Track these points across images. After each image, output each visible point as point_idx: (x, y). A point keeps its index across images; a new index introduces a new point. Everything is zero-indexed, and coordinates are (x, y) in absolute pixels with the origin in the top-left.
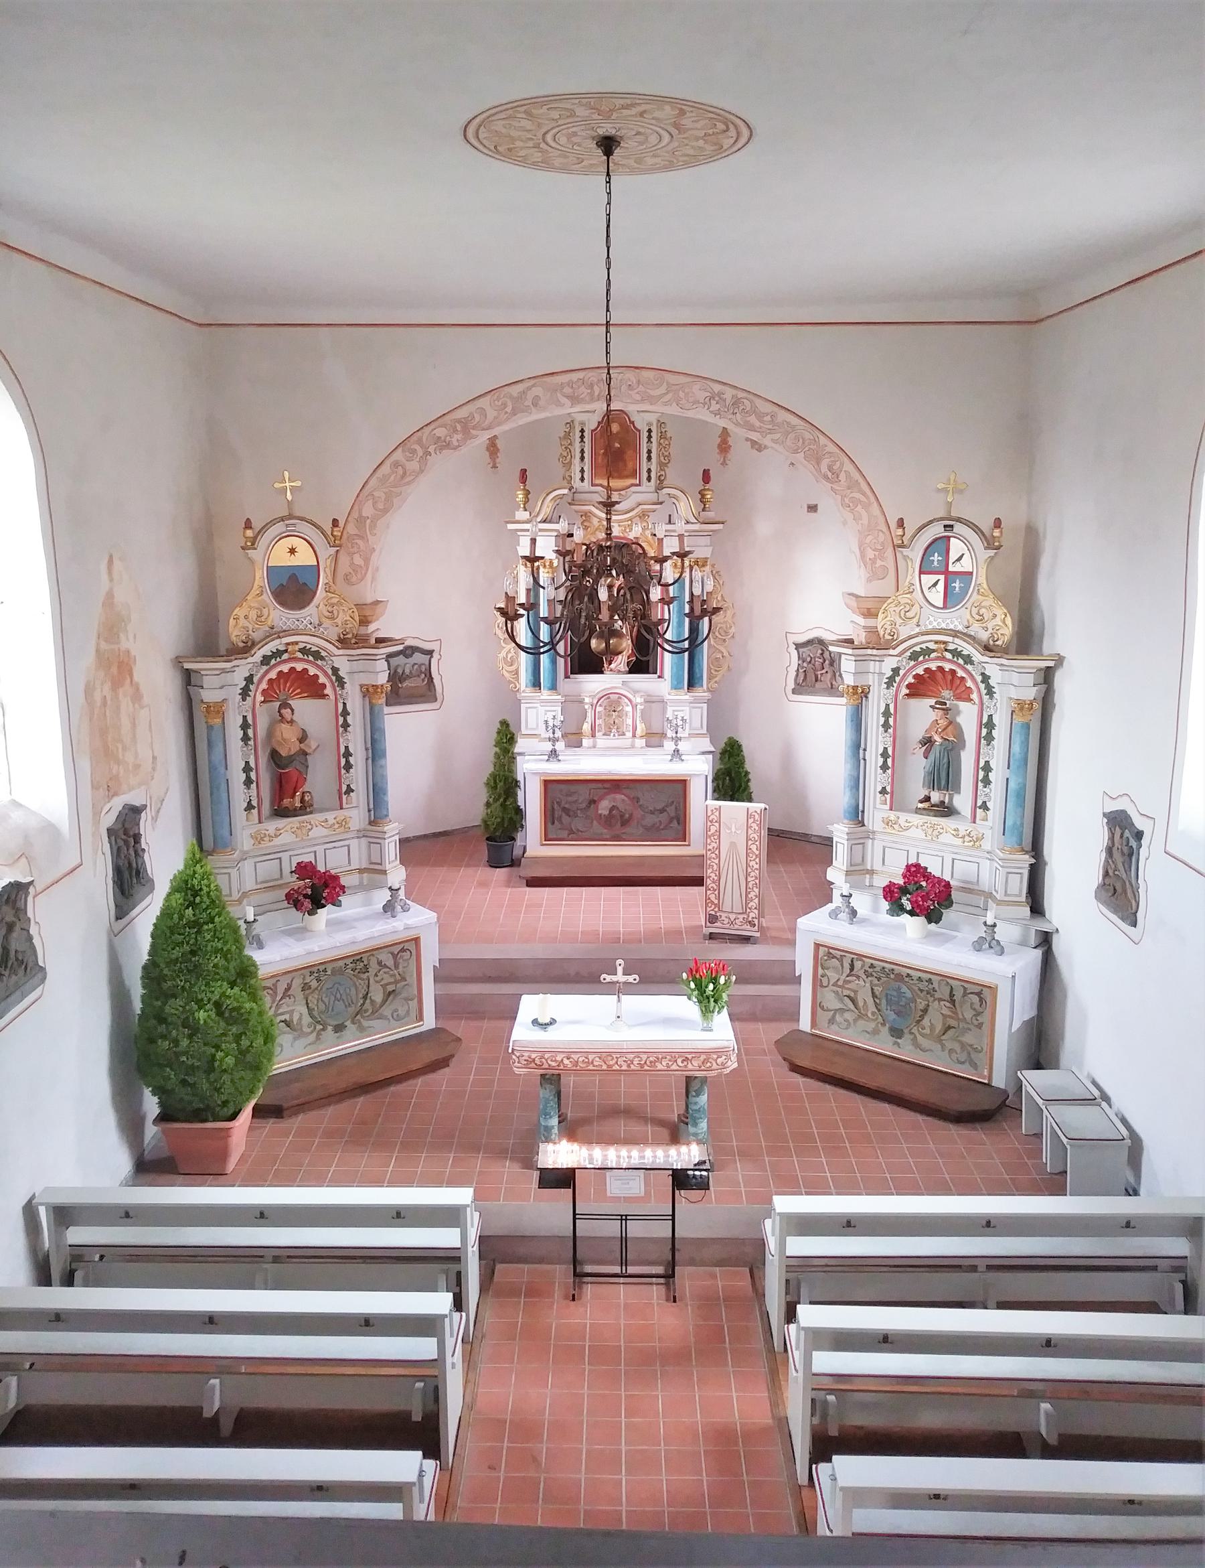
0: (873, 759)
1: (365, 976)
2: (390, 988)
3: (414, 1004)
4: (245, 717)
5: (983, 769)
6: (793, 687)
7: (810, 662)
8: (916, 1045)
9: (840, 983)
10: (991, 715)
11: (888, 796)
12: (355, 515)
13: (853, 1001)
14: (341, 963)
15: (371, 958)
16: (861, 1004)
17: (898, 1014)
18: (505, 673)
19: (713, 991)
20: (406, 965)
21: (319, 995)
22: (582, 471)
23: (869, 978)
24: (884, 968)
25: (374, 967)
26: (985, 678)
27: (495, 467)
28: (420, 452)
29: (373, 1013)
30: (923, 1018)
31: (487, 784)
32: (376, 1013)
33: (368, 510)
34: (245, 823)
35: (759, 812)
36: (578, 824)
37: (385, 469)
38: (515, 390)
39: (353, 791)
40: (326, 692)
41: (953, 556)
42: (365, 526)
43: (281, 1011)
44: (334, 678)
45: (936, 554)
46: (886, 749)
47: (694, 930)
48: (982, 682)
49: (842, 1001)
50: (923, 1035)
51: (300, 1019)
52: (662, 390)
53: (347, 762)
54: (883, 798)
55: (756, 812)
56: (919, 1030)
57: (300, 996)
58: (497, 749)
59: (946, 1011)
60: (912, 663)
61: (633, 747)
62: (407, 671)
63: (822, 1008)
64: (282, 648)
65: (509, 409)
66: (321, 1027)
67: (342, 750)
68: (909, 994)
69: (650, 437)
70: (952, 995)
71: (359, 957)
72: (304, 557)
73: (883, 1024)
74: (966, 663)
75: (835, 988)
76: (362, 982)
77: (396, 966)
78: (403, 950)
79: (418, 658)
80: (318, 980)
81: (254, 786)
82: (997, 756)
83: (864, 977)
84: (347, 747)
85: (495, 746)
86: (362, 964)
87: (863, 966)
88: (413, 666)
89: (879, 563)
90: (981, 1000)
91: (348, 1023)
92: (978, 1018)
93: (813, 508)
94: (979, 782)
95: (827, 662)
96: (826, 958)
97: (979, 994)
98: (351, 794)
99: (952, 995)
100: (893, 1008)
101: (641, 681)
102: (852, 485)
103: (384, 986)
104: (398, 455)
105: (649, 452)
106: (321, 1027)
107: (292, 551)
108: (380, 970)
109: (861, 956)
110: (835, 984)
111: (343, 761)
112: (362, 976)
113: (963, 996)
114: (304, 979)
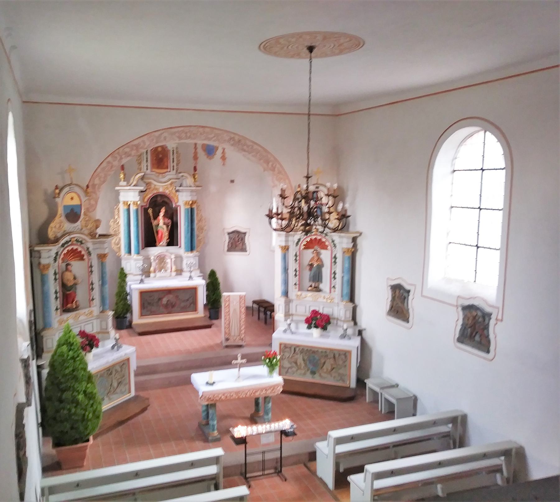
0: (291, 273)
2: (120, 380)
3: (127, 386)
8: (320, 375)
16: (299, 364)
22: (147, 166)
25: (114, 373)
28: (119, 158)
32: (114, 392)
33: (97, 181)
36: (154, 308)
37: (104, 164)
38: (157, 134)
47: (219, 345)
49: (291, 363)
52: (213, 135)
61: (171, 276)
65: (155, 141)
69: (173, 153)
72: (76, 202)
73: (308, 370)
77: (121, 371)
82: (338, 269)
87: (299, 350)
93: (232, 181)
101: (172, 249)
102: (280, 172)
104: (110, 159)
105: (173, 159)
107: (72, 199)
109: (298, 346)
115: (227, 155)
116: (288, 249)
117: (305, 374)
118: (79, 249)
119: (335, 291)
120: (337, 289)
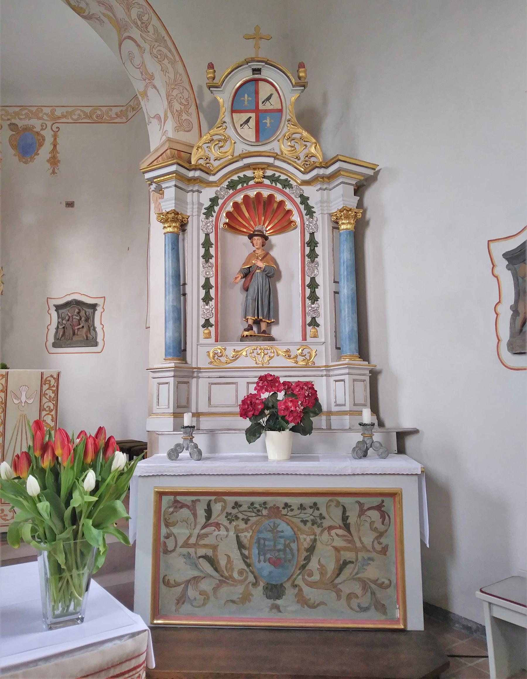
5: (309, 286)
6: (53, 341)
7: (68, 320)
9: (193, 540)
10: (313, 233)
11: (212, 329)
13: (212, 561)
16: (223, 562)
17: (275, 563)
19: (93, 493)
23: (234, 523)
24: (252, 504)
26: (304, 200)
30: (309, 561)
35: (55, 376)
41: (262, 96)
45: (246, 96)
46: (207, 280)
48: (301, 203)
49: (195, 566)
50: (311, 585)
54: (207, 331)
55: (52, 376)
56: (304, 579)
59: (339, 543)
60: (231, 192)
63: (167, 584)
68: (288, 531)
70: (345, 518)
73: (255, 584)
74: (284, 186)
75: (185, 551)
83: (226, 523)
87: (224, 508)
89: (184, 117)
90: (383, 515)
92: (381, 540)
93: (70, 205)
94: (307, 300)
95: (83, 319)
96: (171, 510)
97: (379, 508)
99: (345, 518)
100: (268, 556)
110: (186, 544)
113: (359, 516)
115: (59, 156)
116: (183, 226)
117: (246, 598)
119: (315, 336)
120: (321, 330)
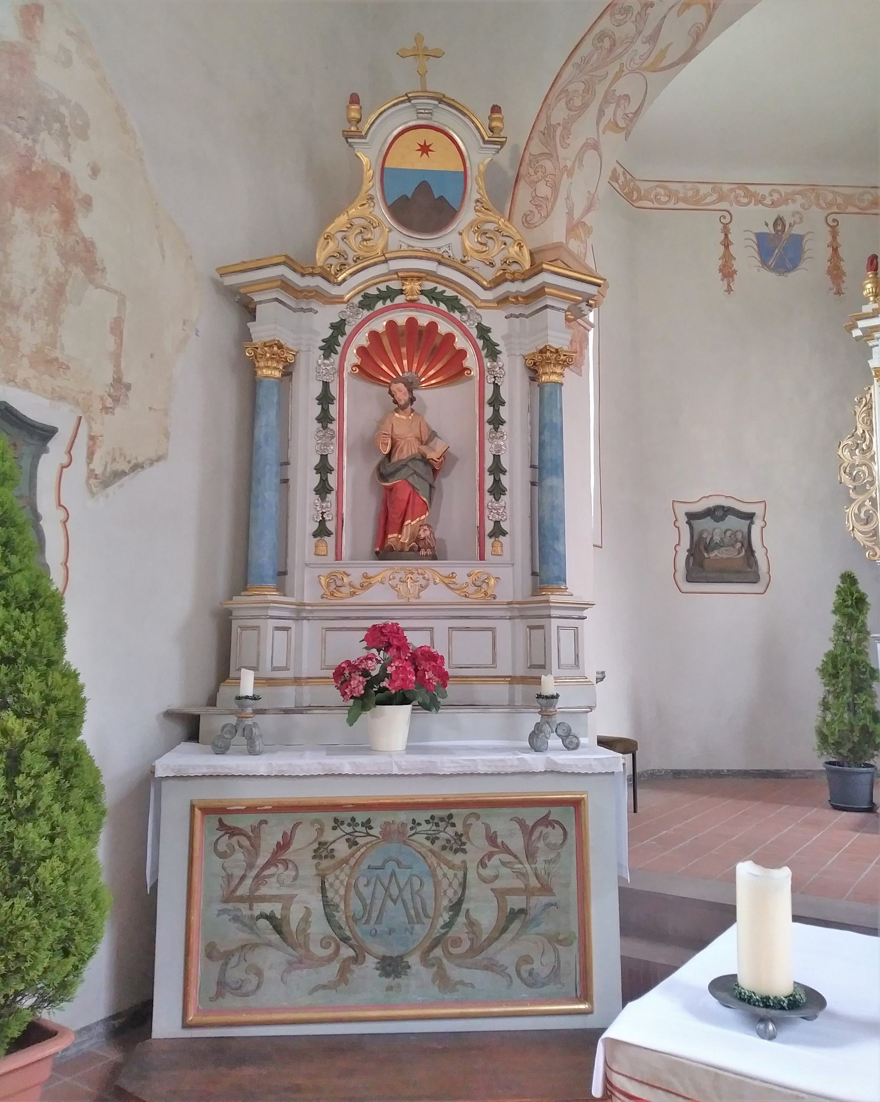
1: (458, 859)
2: (516, 902)
4: (326, 385)
12: (541, 126)
14: (403, 817)
15: (472, 820)
18: (858, 536)
20: (552, 856)
21: (350, 876)
25: (477, 845)
27: (839, 292)
29: (475, 950)
31: (823, 671)
34: (310, 557)
39: (504, 533)
40: (467, 363)
42: (554, 138)
43: (264, 891)
44: (480, 343)
51: (306, 920)
53: (497, 482)
57: (308, 869)
58: (835, 619)
62: (717, 539)
64: (395, 285)
66: (351, 953)
67: (489, 462)
71: (444, 813)
76: (450, 873)
78: (545, 821)
79: (732, 522)
80: (352, 843)
81: (332, 497)
84: (497, 458)
85: (834, 612)
86: (450, 830)
88: (725, 533)
91: (414, 960)
98: (501, 538)
103: (501, 894)
106: (351, 953)
108: (490, 855)
111: (489, 481)
112: (449, 856)
114: (321, 831)
118: (444, 328)
